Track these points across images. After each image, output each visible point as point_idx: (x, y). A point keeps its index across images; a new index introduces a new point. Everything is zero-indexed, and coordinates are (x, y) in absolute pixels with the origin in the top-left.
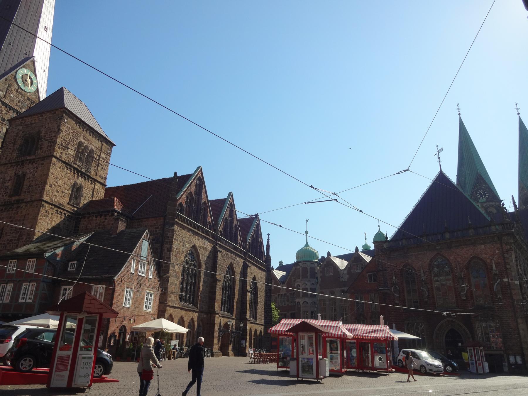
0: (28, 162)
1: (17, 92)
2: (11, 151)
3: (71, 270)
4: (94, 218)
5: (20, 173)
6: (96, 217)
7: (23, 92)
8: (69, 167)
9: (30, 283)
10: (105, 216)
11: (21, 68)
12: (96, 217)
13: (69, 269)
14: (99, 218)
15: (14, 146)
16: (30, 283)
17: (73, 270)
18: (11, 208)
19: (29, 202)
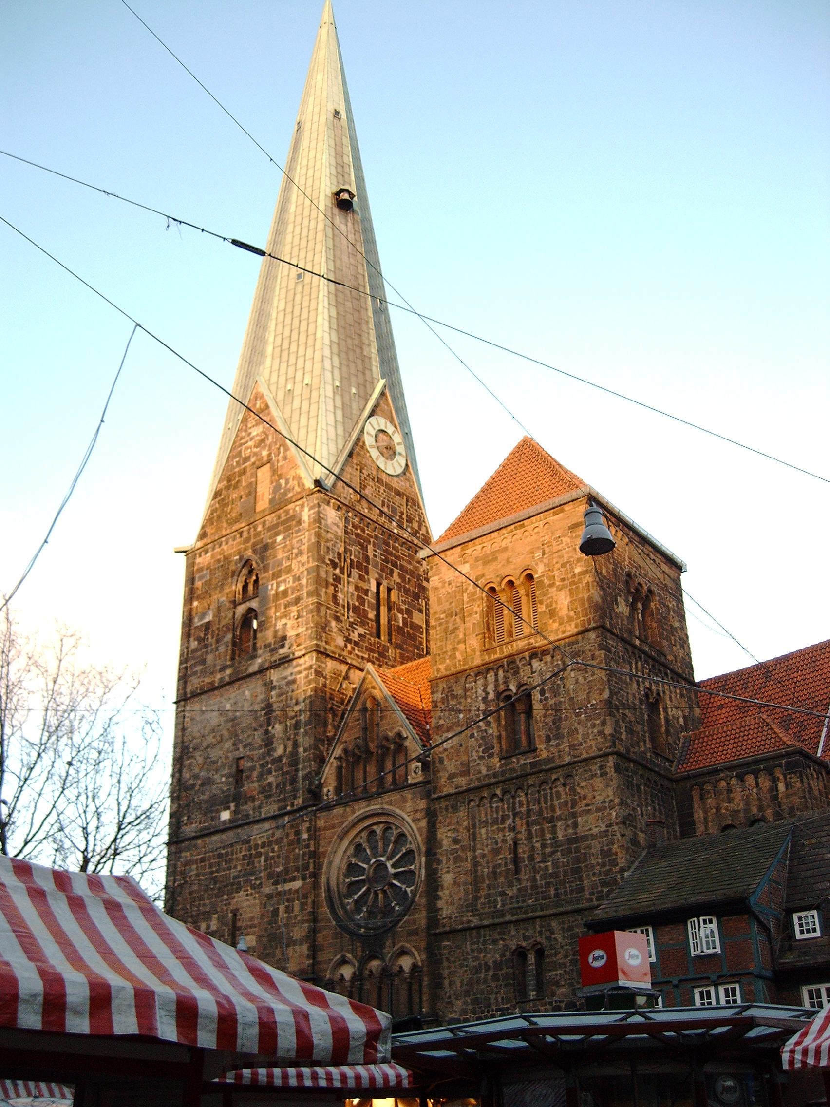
0: (527, 654)
1: (373, 480)
2: (461, 636)
3: (806, 936)
4: (734, 781)
5: (513, 688)
6: (741, 778)
7: (384, 477)
8: (628, 647)
9: (716, 985)
10: (770, 772)
11: (369, 417)
12: (741, 778)
13: (798, 936)
14: (750, 779)
15: (463, 619)
16: (716, 985)
17: (812, 935)
18: (520, 788)
19: (569, 764)
